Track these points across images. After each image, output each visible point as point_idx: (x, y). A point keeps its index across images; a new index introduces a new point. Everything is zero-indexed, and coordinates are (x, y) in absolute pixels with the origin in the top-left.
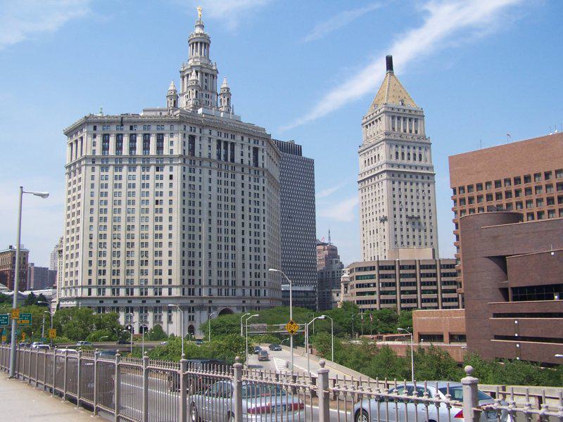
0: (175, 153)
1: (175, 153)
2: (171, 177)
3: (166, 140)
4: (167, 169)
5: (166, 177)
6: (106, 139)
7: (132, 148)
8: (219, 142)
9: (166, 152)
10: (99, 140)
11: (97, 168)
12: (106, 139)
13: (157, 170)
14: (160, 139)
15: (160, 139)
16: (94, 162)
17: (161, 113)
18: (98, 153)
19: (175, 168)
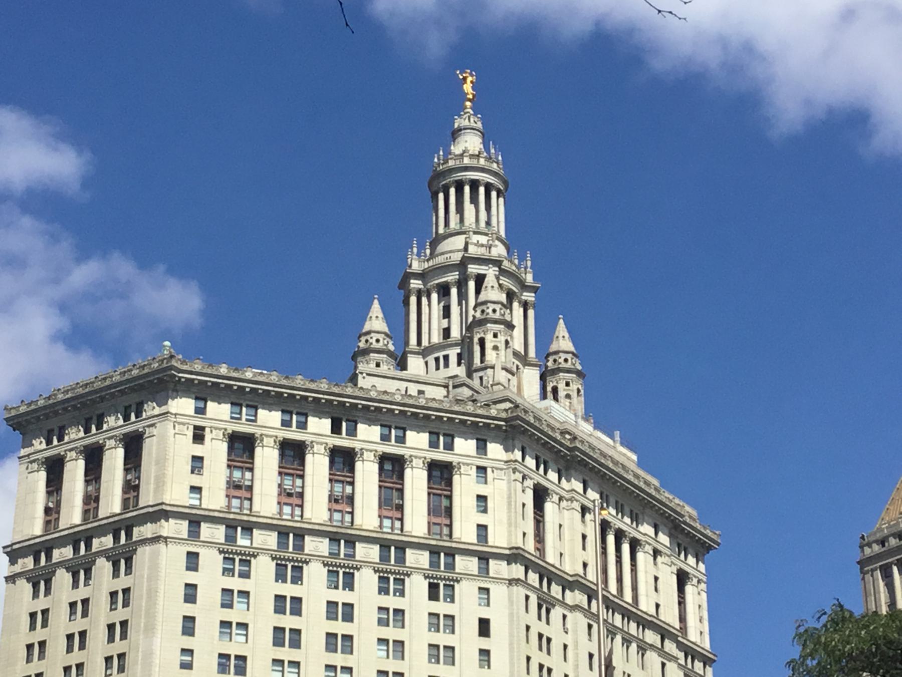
0: (498, 539)
1: (498, 539)
2: (484, 627)
3: (465, 487)
4: (467, 591)
5: (468, 627)
6: (242, 447)
7: (343, 502)
8: (605, 526)
9: (464, 531)
10: (216, 451)
11: (211, 560)
12: (242, 447)
13: (433, 595)
14: (441, 474)
15: (441, 474)
16: (194, 533)
17: (421, 392)
18: (215, 499)
19: (498, 592)
